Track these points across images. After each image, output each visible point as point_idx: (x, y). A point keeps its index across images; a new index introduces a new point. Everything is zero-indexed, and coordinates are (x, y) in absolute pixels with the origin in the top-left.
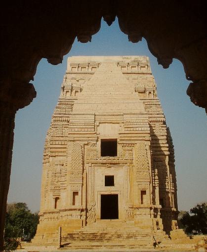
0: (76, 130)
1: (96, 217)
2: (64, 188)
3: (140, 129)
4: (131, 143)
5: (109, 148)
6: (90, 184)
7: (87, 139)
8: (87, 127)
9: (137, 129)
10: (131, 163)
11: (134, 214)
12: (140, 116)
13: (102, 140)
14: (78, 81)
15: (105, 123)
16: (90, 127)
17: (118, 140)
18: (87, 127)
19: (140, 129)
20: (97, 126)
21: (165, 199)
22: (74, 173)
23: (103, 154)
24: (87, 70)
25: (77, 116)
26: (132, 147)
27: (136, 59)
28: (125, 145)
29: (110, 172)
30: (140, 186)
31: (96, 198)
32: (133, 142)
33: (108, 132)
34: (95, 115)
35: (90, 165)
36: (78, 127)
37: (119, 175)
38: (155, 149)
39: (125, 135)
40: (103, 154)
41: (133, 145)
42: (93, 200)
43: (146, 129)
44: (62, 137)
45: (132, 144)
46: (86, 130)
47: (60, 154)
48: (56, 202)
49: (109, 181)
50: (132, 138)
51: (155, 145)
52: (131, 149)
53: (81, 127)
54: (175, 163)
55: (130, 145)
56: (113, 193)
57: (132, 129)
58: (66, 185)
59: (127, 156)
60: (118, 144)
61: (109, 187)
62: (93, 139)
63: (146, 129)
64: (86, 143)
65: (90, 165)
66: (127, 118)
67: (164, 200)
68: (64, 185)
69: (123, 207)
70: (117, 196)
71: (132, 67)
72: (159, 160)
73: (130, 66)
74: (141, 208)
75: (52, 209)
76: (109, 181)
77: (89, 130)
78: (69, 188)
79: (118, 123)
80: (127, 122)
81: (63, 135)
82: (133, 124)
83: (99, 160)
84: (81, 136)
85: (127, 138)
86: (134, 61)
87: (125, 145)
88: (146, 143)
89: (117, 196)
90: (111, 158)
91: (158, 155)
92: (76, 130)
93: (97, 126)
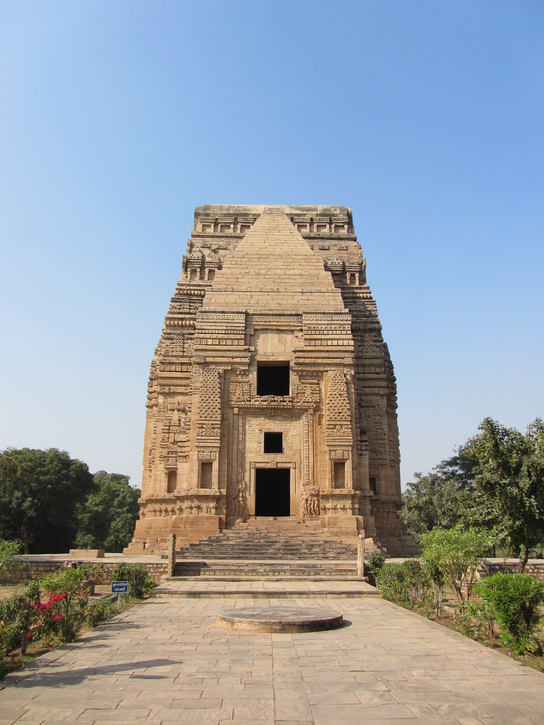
0: (210, 342)
2: (184, 454)
3: (335, 343)
5: (274, 378)
7: (231, 360)
8: (232, 336)
9: (330, 343)
10: (317, 409)
11: (321, 506)
12: (336, 317)
14: (215, 251)
16: (238, 337)
17: (292, 364)
18: (232, 336)
19: (335, 343)
20: (251, 335)
21: (379, 479)
22: (205, 426)
23: (261, 391)
24: (231, 230)
25: (212, 316)
27: (327, 212)
29: (274, 426)
32: (321, 369)
33: (273, 348)
34: (247, 314)
36: (214, 336)
38: (361, 383)
39: (306, 355)
40: (261, 391)
41: (320, 374)
43: (346, 342)
44: (183, 357)
45: (318, 371)
46: (229, 342)
47: (180, 390)
48: (169, 481)
49: (273, 443)
50: (319, 361)
51: (361, 376)
52: (316, 381)
53: (220, 336)
54: (397, 411)
56: (280, 465)
57: (318, 343)
58: (188, 449)
59: (308, 395)
60: (291, 372)
62: (243, 360)
63: (346, 342)
66: (307, 320)
67: (377, 480)
68: (184, 449)
69: (298, 492)
70: (286, 472)
71: (318, 226)
72: (368, 404)
73: (315, 225)
75: (162, 493)
76: (273, 443)
77: (236, 342)
78: (194, 455)
79: (292, 331)
80: (309, 329)
81: (185, 354)
82: (321, 332)
83: (252, 402)
85: (307, 361)
86: (323, 215)
87: (305, 373)
88: (346, 370)
89: (286, 472)
90: (278, 398)
91: (367, 394)
92: (210, 342)
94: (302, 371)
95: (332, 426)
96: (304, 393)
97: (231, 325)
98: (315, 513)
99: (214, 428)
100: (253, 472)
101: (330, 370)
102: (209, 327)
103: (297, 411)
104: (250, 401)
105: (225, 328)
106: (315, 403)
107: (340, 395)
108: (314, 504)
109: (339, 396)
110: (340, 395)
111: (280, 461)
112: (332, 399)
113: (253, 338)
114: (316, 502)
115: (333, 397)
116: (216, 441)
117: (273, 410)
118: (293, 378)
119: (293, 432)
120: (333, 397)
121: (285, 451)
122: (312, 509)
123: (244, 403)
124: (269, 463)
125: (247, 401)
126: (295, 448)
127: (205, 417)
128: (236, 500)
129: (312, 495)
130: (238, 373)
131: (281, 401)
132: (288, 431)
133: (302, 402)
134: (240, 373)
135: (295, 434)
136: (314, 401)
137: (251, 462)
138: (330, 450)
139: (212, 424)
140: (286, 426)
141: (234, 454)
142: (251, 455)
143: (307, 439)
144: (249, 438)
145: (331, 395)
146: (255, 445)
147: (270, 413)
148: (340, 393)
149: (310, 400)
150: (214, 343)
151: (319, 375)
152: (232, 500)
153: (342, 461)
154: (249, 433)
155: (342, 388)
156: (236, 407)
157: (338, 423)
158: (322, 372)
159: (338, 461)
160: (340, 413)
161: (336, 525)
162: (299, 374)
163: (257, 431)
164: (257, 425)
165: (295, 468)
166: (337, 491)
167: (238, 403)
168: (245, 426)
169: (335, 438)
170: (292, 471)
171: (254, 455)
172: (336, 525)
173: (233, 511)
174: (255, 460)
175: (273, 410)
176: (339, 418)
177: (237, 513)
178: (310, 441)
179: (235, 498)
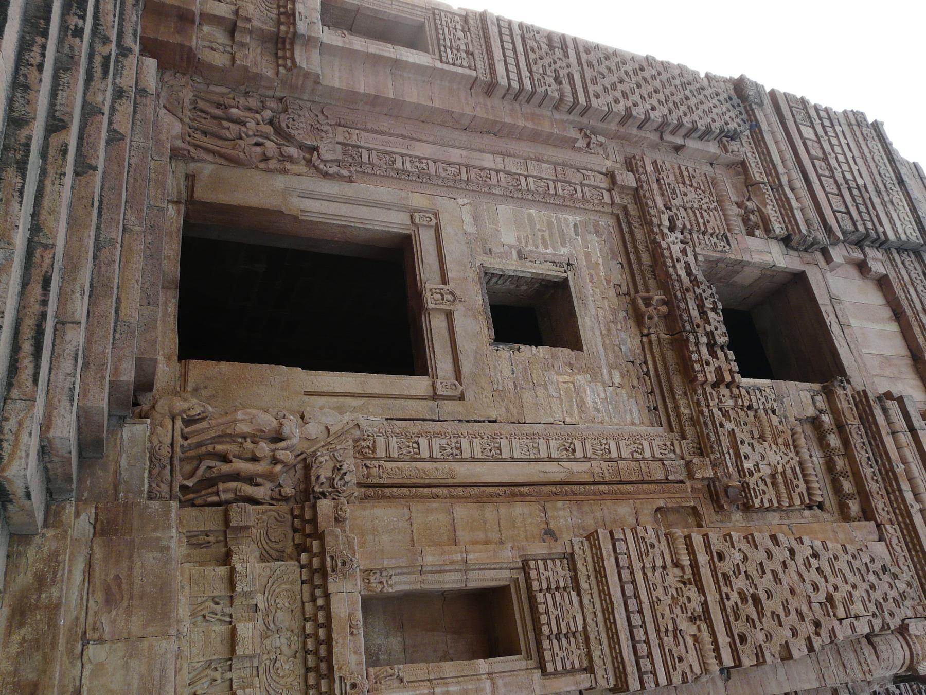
0: (808, 133)
1: (207, 169)
4: (873, 487)
6: (488, 161)
11: (241, 514)
13: (800, 278)
15: (898, 315)
26: (830, 501)
28: (834, 440)
30: (559, 574)
31: (383, 192)
35: (628, 179)
37: (587, 399)
41: (854, 507)
42: (353, 165)
45: (864, 496)
55: (847, 486)
56: (436, 325)
61: (477, 298)
64: (757, 173)
65: (628, 179)
69: (318, 408)
74: (318, 577)
84: (789, 155)
93: (862, 267)
94: (841, 428)
95: (685, 561)
96: (762, 438)
97: (876, 201)
98: (195, 489)
99: (557, 80)
100: (393, 221)
101: (889, 546)
102: (843, 141)
103: (685, 411)
104: (672, 229)
105: (860, 182)
106: (745, 487)
107: (830, 599)
108: (250, 480)
109: (822, 597)
110: (830, 599)
111: (458, 328)
112: (799, 559)
113: (853, 272)
114: (259, 492)
115: (808, 565)
116: (514, 76)
117: (664, 309)
118: (798, 397)
119: (594, 394)
120: (808, 565)
121: (505, 352)
122: (225, 468)
123: (660, 205)
124: (445, 281)
125: (671, 220)
126: (527, 396)
127: (590, 64)
128: (269, 129)
129: (307, 465)
130: (750, 205)
131: (710, 335)
132: (593, 373)
133: (729, 426)
134: (748, 212)
135: (589, 400)
136: (751, 481)
137: (436, 215)
138: (571, 558)
139: (570, 77)
140: (611, 367)
141: (464, 153)
142: (468, 219)
143: (579, 454)
144: (530, 217)
145: (815, 555)
146: (509, 237)
147: (647, 302)
148: (837, 596)
149: (748, 465)
150: (809, 143)
151: (851, 500)
152: (268, 114)
153: (523, 634)
154: (550, 224)
155: (857, 608)
156: (638, 180)
157: (712, 598)
158: (867, 514)
159: (519, 610)
160: (756, 601)
161: (110, 601)
162: (826, 418)
163: (563, 251)
164: (588, 255)
165: (435, 397)
166: (346, 598)
167: (655, 186)
168: (574, 209)
169: (639, 576)
170: (417, 384)
171: (470, 228)
172: (110, 601)
173: (218, 112)
174: (448, 230)
175: (664, 309)
176: (735, 597)
177: (210, 125)
178: (575, 467)
179: (278, 131)
